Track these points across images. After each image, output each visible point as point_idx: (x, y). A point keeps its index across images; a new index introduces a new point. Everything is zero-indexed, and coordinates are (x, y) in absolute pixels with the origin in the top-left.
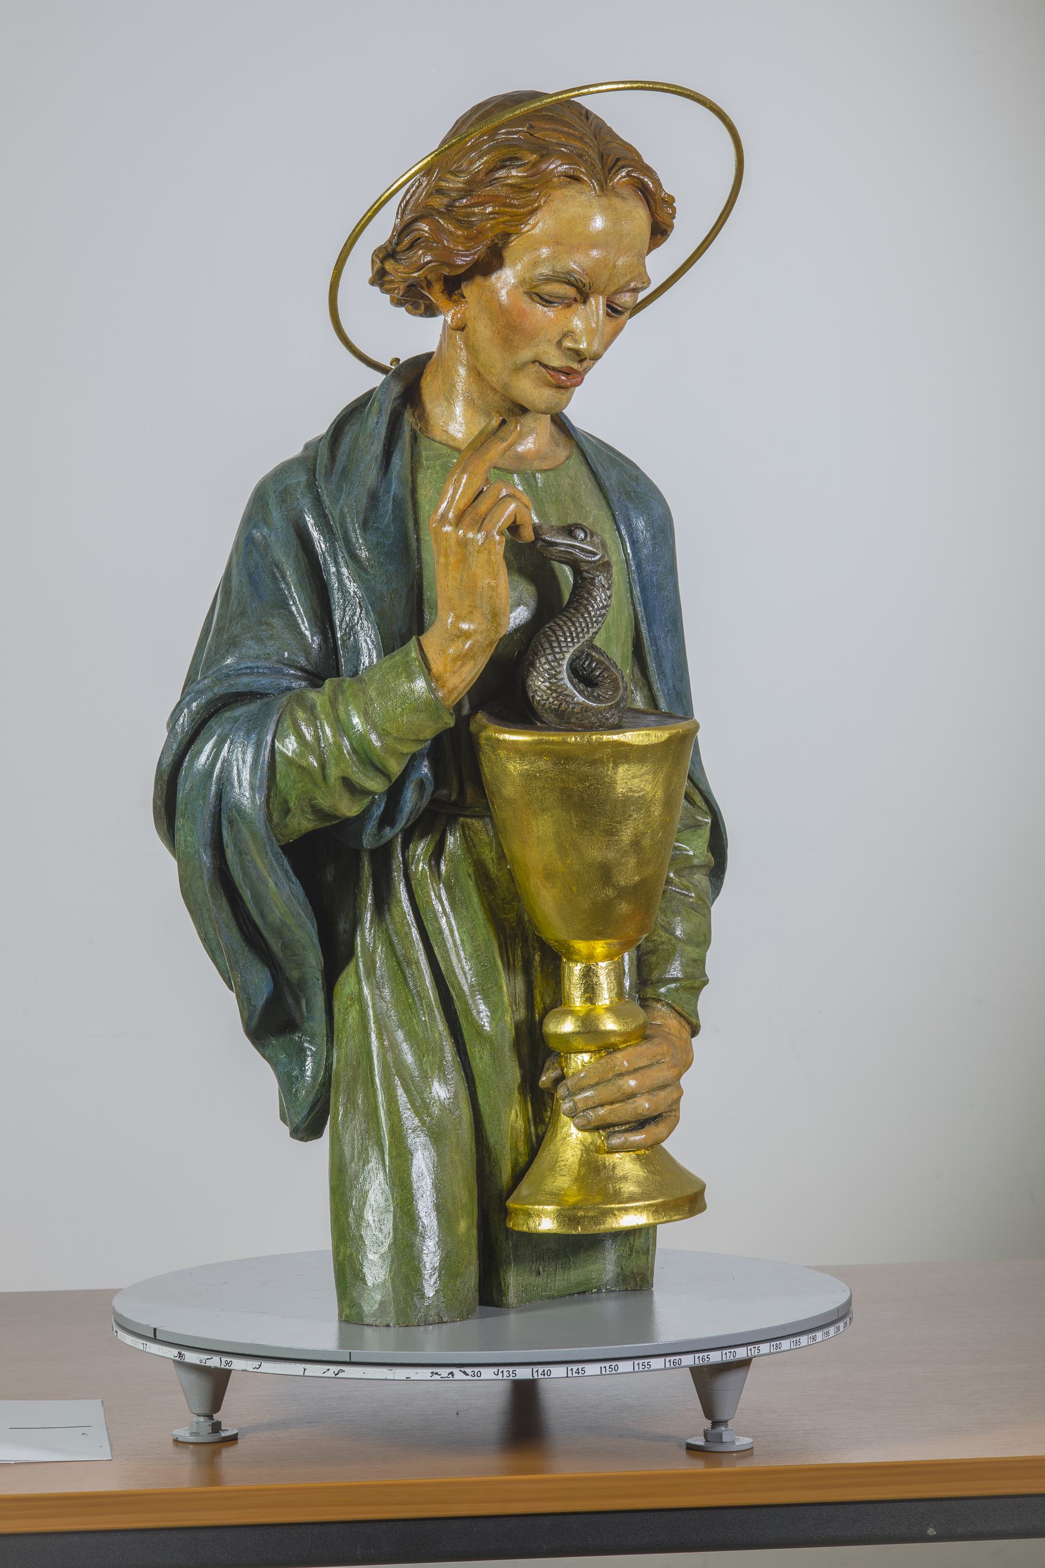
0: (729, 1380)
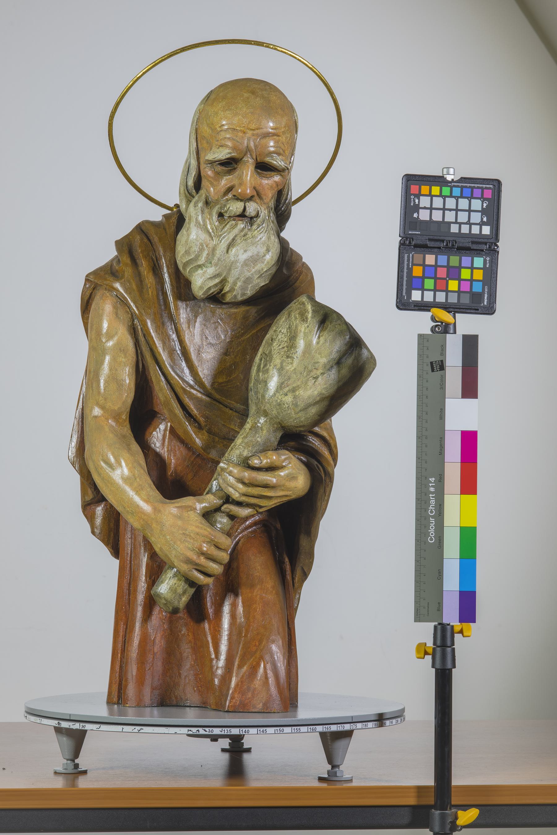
0: (341, 743)
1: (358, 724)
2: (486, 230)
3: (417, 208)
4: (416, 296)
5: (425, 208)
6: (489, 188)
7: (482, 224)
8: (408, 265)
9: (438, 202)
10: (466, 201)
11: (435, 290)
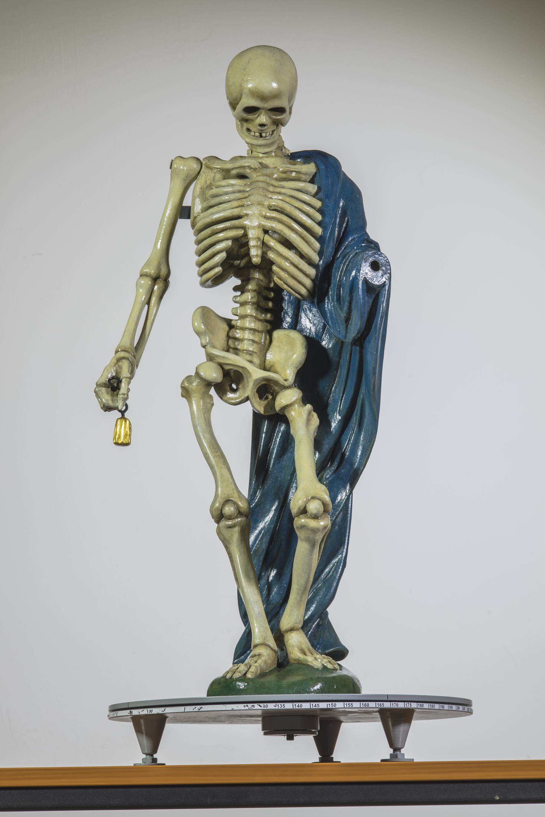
1: (412, 703)
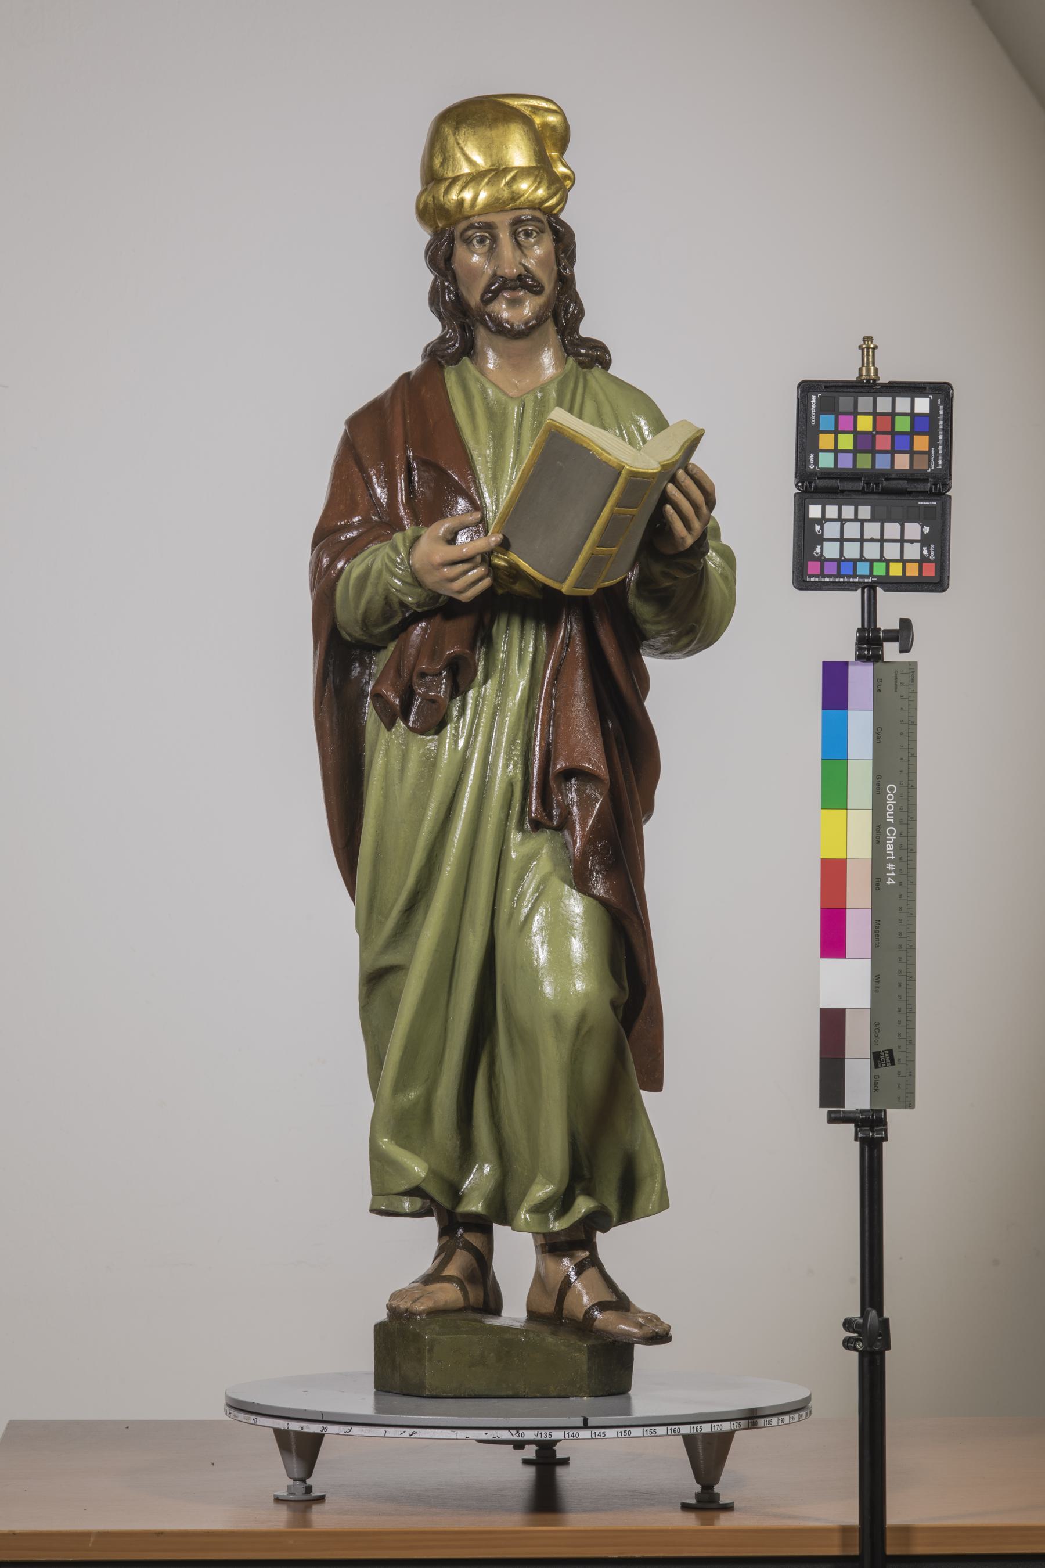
2: (815, 511)
3: (924, 541)
4: (923, 405)
5: (912, 541)
6: (811, 576)
7: (822, 521)
8: (937, 452)
9: (892, 551)
10: (847, 555)
11: (893, 415)
